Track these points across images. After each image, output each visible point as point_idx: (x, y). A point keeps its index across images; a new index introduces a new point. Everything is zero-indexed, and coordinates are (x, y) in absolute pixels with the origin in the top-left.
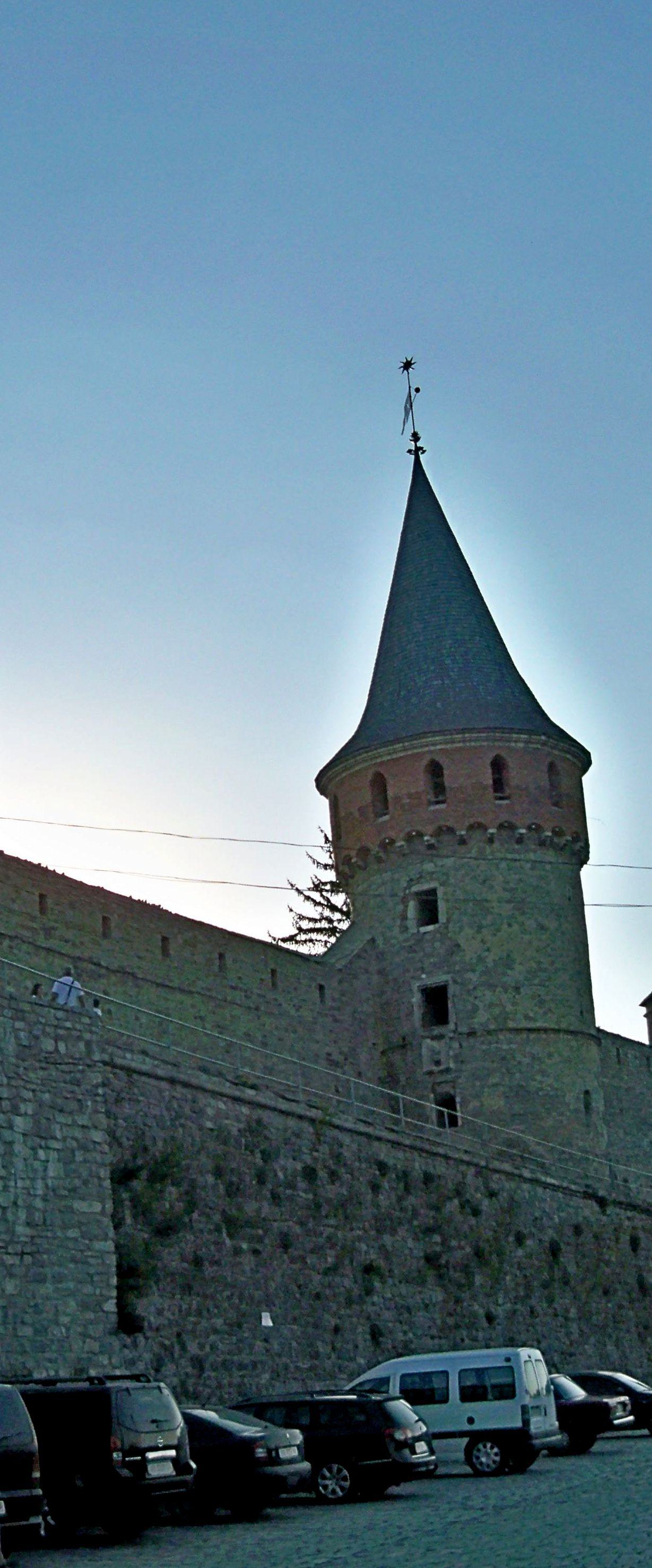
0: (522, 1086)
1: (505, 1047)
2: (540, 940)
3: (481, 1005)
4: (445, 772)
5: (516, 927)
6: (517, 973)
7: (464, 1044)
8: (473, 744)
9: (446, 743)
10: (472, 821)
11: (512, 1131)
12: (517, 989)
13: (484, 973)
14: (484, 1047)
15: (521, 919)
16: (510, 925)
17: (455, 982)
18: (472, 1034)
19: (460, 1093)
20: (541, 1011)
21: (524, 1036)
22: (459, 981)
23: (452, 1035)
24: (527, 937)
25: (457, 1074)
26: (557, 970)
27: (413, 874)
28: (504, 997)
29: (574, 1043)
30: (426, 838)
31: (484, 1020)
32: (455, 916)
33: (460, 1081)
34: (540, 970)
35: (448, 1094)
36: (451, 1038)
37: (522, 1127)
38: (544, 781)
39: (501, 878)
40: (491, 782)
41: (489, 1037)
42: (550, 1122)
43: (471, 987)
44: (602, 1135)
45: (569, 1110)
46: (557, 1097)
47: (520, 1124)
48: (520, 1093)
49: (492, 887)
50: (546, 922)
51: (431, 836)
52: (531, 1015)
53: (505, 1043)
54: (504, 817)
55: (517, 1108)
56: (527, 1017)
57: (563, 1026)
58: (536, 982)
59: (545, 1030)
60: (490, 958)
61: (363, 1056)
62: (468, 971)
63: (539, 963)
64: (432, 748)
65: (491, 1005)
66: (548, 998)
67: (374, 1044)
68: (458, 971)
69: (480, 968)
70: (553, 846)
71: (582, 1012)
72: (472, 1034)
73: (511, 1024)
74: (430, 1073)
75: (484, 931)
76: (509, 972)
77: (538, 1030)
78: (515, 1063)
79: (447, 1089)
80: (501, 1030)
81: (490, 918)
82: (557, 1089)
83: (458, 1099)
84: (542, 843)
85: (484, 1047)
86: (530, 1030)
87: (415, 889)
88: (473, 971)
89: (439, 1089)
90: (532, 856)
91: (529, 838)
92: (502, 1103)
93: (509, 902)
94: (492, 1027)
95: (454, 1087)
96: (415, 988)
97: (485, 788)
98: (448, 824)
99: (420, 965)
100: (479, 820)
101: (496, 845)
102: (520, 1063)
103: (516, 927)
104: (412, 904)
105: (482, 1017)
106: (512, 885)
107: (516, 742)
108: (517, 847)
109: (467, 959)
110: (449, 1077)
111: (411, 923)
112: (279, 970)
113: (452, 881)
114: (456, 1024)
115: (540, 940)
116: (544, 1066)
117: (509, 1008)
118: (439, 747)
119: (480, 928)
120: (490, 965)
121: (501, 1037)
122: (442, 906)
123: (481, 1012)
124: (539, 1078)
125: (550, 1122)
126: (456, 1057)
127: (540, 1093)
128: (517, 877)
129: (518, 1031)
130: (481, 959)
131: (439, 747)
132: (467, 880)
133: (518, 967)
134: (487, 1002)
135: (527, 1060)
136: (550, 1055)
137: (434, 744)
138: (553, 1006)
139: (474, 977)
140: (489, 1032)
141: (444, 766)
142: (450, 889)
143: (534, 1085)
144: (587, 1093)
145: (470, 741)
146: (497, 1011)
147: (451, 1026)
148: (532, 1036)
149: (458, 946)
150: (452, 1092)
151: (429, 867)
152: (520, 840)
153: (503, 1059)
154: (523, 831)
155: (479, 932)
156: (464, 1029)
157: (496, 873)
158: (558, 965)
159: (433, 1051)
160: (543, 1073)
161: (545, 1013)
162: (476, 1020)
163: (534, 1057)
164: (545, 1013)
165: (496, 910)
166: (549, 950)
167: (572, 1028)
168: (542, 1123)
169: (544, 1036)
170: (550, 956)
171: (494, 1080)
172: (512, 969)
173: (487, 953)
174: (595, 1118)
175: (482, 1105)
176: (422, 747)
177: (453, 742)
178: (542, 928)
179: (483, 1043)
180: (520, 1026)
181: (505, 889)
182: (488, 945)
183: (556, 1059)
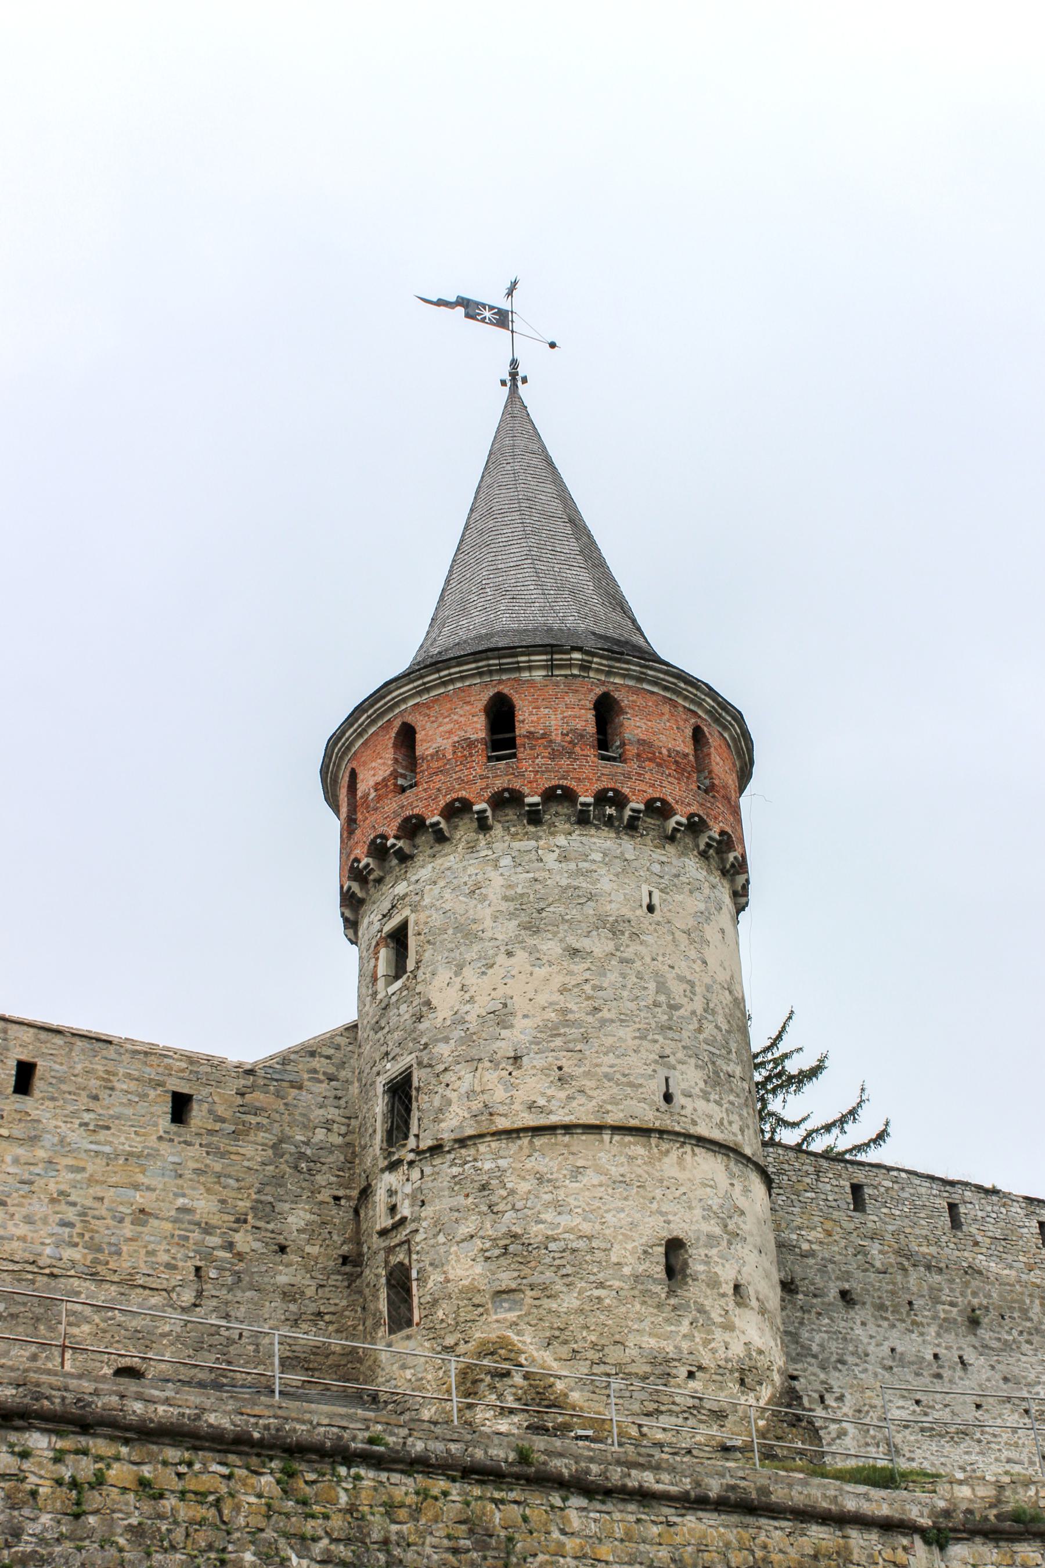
0: (515, 1236)
1: (488, 1165)
2: (570, 973)
3: (453, 1096)
4: (417, 736)
5: (521, 956)
6: (520, 1033)
7: (428, 1170)
8: (459, 685)
9: (419, 693)
10: (449, 798)
11: (495, 1324)
12: (516, 1059)
13: (461, 1041)
14: (455, 1170)
15: (531, 941)
16: (509, 954)
17: (420, 1064)
18: (437, 1149)
19: (418, 1261)
20: (562, 1095)
21: (525, 1141)
22: (425, 1062)
23: (411, 1156)
24: (540, 972)
25: (413, 1226)
26: (603, 1022)
27: (386, 905)
28: (491, 1077)
29: (637, 1148)
30: (389, 843)
31: (455, 1123)
32: (427, 956)
33: (419, 1238)
34: (567, 1023)
35: (401, 1264)
36: (411, 1163)
37: (512, 1316)
38: (586, 721)
39: (498, 881)
40: (482, 735)
41: (463, 1151)
42: (570, 1301)
43: (441, 1067)
44: (729, 1327)
45: (622, 1278)
46: (592, 1250)
47: (510, 1310)
48: (512, 1248)
49: (484, 898)
50: (585, 944)
51: (396, 837)
52: (542, 1102)
53: (488, 1158)
54: (499, 784)
55: (506, 1279)
56: (531, 1106)
57: (610, 1120)
58: (558, 1042)
59: (568, 1128)
60: (473, 1013)
61: (297, 1218)
62: (437, 1041)
63: (565, 1011)
64: (403, 707)
65: (470, 1094)
66: (579, 1071)
67: (337, 1198)
68: (426, 1046)
69: (457, 1033)
70: (609, 822)
71: (668, 1098)
72: (437, 1149)
73: (502, 1123)
74: (383, 1233)
75: (467, 971)
76: (505, 1033)
77: (551, 1129)
78: (504, 1193)
79: (401, 1256)
80: (481, 1136)
81: (476, 948)
82: (590, 1238)
83: (414, 1274)
84: (583, 820)
85: (455, 1170)
86: (537, 1131)
87: (387, 928)
88: (446, 1040)
89: (394, 1260)
90: (561, 840)
91: (557, 814)
92: (478, 1269)
93: (512, 915)
94: (470, 1132)
95: (409, 1252)
96: (380, 1089)
97: (471, 744)
98: (416, 811)
99: (384, 1049)
100: (463, 794)
101: (498, 830)
102: (512, 1192)
103: (521, 956)
104: (383, 952)
105: (455, 1120)
106: (519, 890)
107: (530, 668)
108: (531, 829)
109: (440, 1020)
110: (402, 1234)
111: (381, 983)
112: (41, 1064)
113: (427, 901)
114: (417, 1136)
115: (570, 973)
116: (561, 1194)
117: (500, 1094)
118: (411, 703)
119: (460, 967)
120: (473, 1027)
121: (482, 1148)
122: (412, 942)
123: (454, 1108)
124: (548, 1216)
125: (570, 1301)
126: (413, 1197)
127: (552, 1246)
128: (531, 875)
129: (511, 1134)
130: (459, 1020)
131: (411, 703)
132: (447, 894)
133: (519, 1023)
134: (463, 1090)
135: (524, 1187)
136: (577, 1172)
137: (404, 700)
138: (589, 1084)
139: (443, 1050)
140: (462, 1142)
141: (418, 729)
142: (422, 917)
143: (536, 1231)
144: (674, 1246)
145: (452, 681)
146: (476, 1106)
147: (412, 1143)
148: (538, 1142)
149: (428, 1003)
150: (406, 1261)
151: (401, 888)
152: (534, 817)
153: (484, 1187)
154: (536, 799)
155: (457, 974)
156: (426, 1143)
157: (492, 874)
158: (605, 1014)
159: (391, 1193)
160: (558, 1206)
161: (570, 1098)
162: (443, 1125)
163: (540, 1179)
164: (570, 1098)
165: (488, 934)
166: (587, 988)
167: (633, 1123)
168: (554, 1306)
169: (567, 1138)
170: (588, 998)
171: (464, 1230)
172: (512, 1026)
173: (468, 1007)
174: (695, 1292)
175: (447, 1281)
176: (391, 709)
177: (428, 690)
178: (574, 952)
179: (453, 1164)
180: (519, 1124)
181: (506, 899)
182: (471, 993)
183: (591, 1178)
